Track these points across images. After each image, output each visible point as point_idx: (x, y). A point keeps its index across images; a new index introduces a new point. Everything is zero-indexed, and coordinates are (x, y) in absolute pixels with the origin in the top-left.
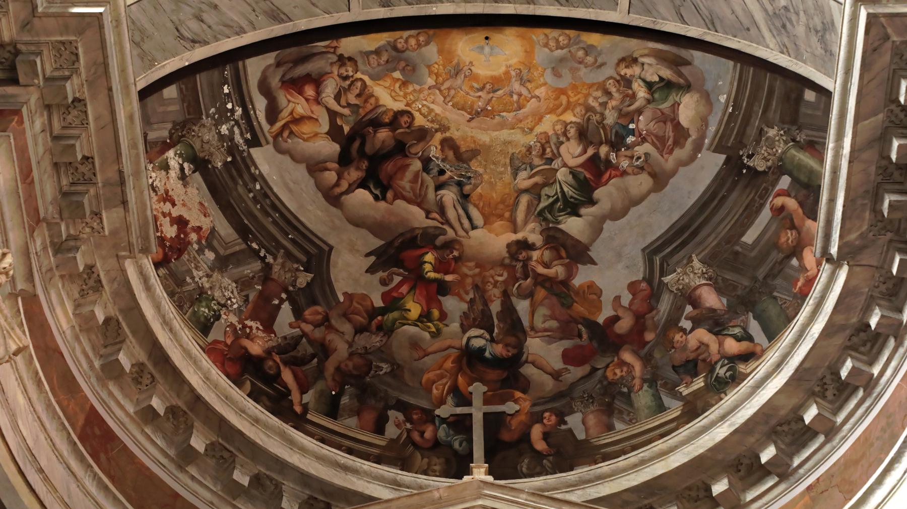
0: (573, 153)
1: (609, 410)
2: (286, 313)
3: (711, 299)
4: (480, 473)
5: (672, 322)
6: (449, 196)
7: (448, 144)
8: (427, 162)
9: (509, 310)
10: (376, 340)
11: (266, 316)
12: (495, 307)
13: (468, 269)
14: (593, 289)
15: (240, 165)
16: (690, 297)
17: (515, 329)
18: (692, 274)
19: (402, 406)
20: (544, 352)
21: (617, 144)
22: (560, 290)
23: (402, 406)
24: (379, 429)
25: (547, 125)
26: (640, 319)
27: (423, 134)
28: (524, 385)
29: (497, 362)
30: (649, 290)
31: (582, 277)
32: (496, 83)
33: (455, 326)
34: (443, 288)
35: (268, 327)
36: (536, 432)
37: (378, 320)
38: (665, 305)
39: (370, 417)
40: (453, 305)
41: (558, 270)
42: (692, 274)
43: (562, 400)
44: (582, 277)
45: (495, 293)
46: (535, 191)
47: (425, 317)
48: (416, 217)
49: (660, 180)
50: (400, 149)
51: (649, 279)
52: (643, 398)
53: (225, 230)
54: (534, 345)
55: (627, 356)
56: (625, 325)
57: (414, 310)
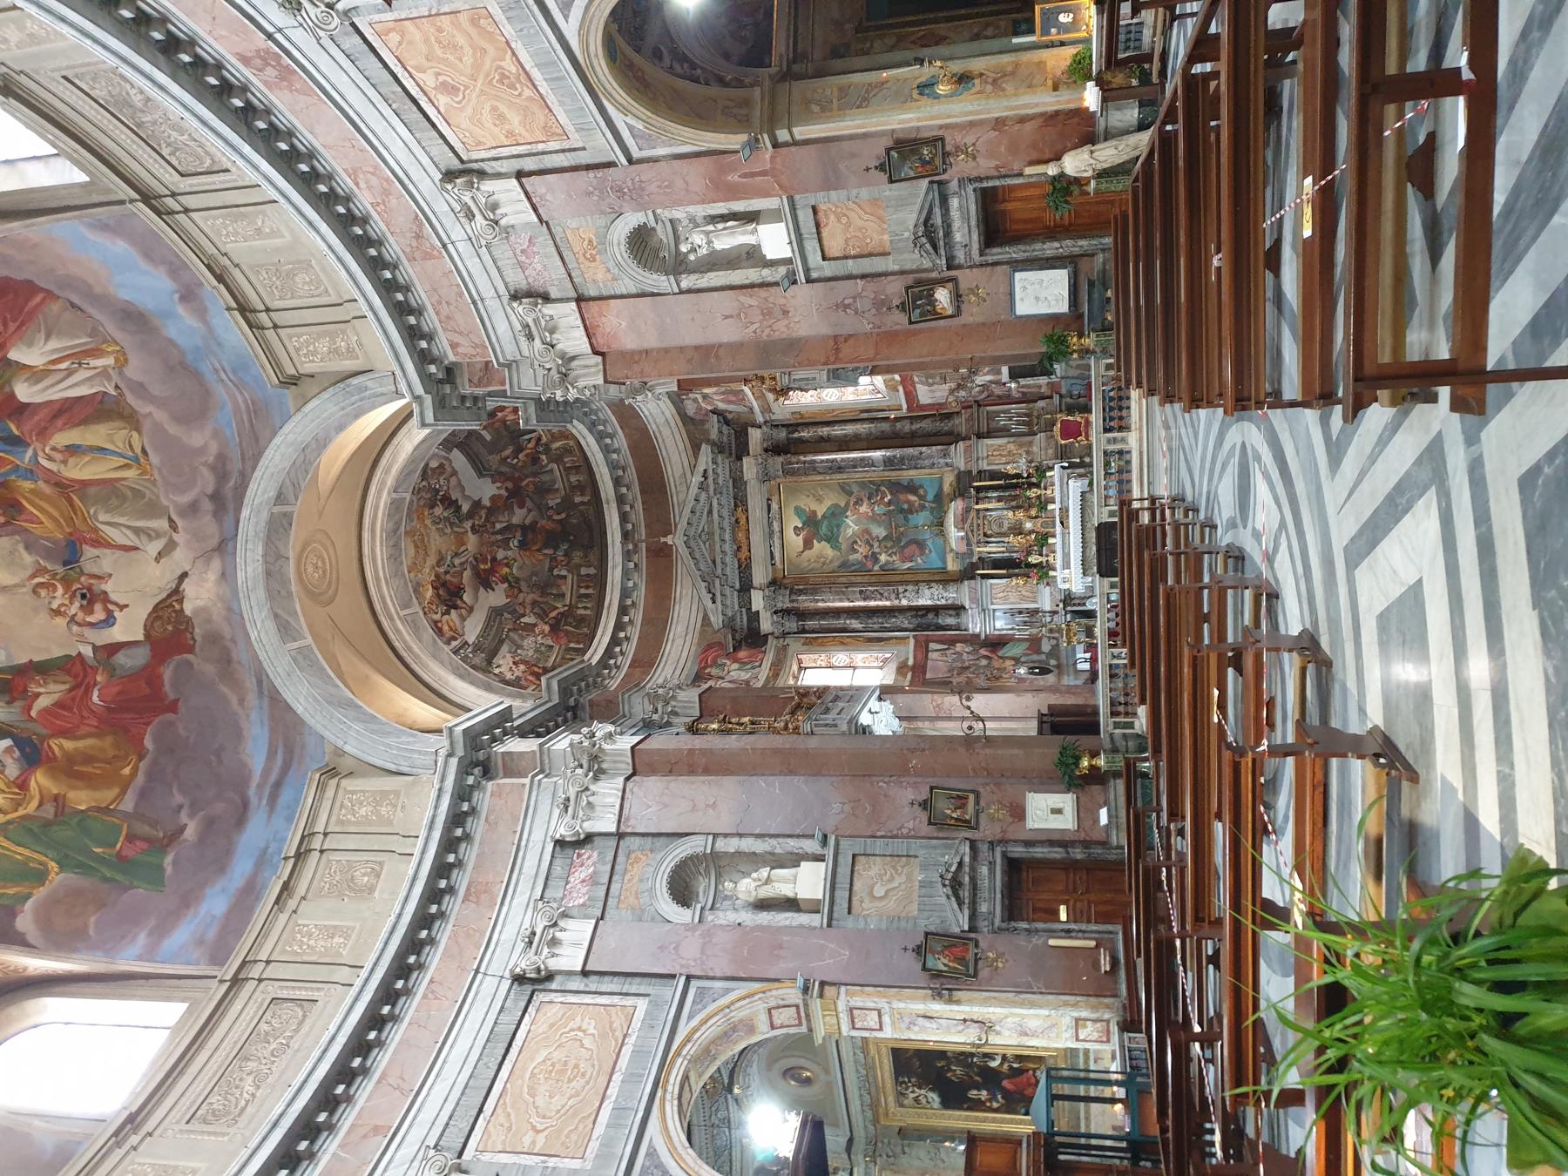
0: (438, 511)
3: (508, 452)
4: (669, 540)
5: (513, 466)
6: (457, 561)
7: (438, 564)
8: (446, 572)
9: (500, 532)
10: (523, 585)
11: (530, 628)
12: (499, 537)
13: (484, 550)
14: (493, 498)
15: (477, 648)
17: (509, 528)
18: (493, 460)
19: (551, 569)
20: (519, 516)
21: (437, 491)
22: (491, 511)
23: (551, 569)
24: (565, 577)
25: (428, 522)
26: (507, 479)
27: (437, 576)
28: (535, 523)
29: (524, 535)
30: (496, 476)
31: (487, 503)
32: (416, 546)
34: (494, 559)
35: (535, 625)
36: (556, 517)
37: (514, 585)
38: (504, 469)
39: (560, 582)
40: (500, 555)
41: (483, 513)
42: (493, 460)
43: (542, 508)
44: (487, 503)
45: (493, 538)
46: (452, 524)
47: (507, 565)
48: (467, 574)
49: (454, 473)
50: (444, 584)
51: (492, 476)
52: (545, 478)
53: (505, 648)
54: (515, 520)
56: (510, 485)
57: (506, 570)
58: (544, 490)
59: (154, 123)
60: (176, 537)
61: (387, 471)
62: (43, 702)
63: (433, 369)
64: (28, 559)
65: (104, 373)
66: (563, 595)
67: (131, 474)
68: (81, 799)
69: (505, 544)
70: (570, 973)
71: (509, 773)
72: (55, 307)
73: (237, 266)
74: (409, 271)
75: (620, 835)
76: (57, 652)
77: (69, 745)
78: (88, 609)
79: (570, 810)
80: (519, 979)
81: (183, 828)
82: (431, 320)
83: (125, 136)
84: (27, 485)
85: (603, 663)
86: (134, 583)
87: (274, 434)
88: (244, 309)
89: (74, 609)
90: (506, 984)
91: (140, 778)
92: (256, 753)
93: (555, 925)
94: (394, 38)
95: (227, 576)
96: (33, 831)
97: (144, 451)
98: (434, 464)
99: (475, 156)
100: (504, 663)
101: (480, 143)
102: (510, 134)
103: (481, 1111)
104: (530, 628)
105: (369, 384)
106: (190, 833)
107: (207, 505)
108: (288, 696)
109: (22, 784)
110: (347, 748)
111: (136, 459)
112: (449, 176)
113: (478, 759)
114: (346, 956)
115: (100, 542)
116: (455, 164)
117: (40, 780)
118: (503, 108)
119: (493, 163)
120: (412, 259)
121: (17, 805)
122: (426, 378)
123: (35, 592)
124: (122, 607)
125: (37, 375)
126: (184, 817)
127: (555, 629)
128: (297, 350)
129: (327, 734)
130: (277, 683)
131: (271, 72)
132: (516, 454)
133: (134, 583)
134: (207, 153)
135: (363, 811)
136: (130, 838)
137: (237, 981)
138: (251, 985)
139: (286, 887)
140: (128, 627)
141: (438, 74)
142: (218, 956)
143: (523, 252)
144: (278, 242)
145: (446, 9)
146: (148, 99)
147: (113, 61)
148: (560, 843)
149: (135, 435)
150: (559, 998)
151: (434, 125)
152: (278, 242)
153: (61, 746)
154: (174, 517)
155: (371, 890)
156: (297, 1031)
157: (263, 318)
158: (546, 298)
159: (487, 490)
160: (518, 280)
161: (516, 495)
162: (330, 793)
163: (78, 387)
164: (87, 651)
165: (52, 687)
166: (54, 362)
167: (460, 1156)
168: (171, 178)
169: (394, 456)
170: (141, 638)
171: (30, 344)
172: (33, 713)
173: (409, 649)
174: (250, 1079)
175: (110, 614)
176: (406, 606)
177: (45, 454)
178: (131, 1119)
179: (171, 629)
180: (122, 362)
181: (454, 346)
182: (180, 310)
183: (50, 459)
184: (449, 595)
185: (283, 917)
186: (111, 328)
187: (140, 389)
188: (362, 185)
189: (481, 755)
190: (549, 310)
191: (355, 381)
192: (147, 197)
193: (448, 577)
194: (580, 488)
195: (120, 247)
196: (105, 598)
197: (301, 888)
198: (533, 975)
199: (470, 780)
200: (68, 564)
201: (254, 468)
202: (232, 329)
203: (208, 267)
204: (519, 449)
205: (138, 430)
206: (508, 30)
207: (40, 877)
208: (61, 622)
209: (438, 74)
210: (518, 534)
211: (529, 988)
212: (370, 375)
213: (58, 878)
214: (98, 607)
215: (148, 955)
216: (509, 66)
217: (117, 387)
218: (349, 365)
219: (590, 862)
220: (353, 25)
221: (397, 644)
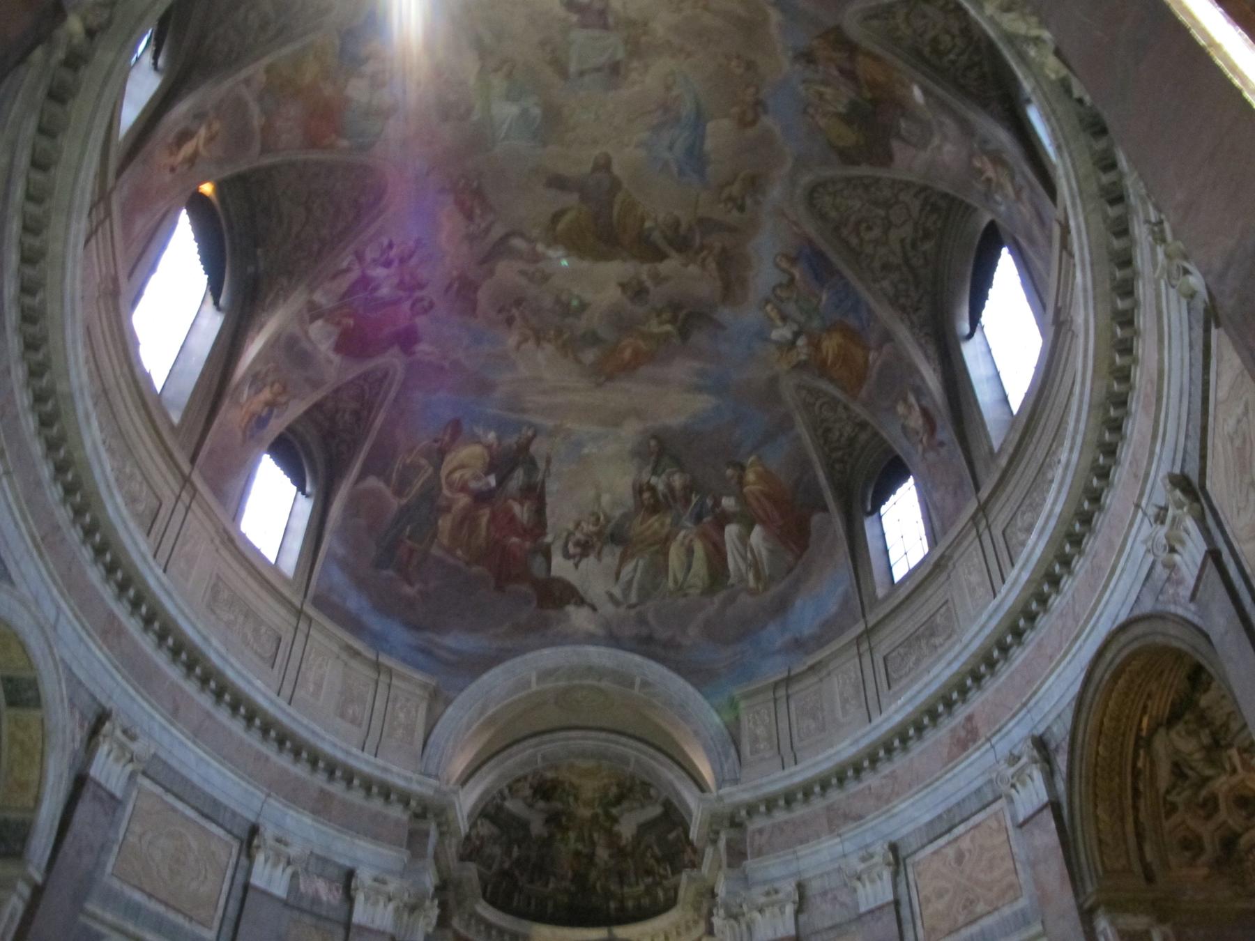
0: (614, 790)
1: (622, 883)
2: (516, 849)
3: (656, 850)
6: (571, 799)
8: (564, 790)
9: (591, 836)
12: (586, 835)
14: (619, 836)
15: (500, 808)
16: (649, 847)
17: (593, 844)
20: (602, 854)
25: (606, 781)
31: (616, 828)
33: (572, 841)
34: (568, 829)
36: (598, 885)
37: (547, 842)
38: (642, 846)
40: (572, 835)
41: (607, 824)
49: (643, 806)
53: (495, 830)
55: (630, 860)
56: (629, 849)
58: (622, 877)
59: (920, 647)
60: (622, 610)
61: (652, 757)
62: (517, 508)
63: (743, 813)
64: (617, 513)
65: (743, 579)
66: (531, 881)
67: (671, 584)
68: (445, 523)
69: (580, 839)
70: (249, 872)
71: (412, 834)
72: (790, 558)
73: (821, 680)
74: (818, 804)
75: (348, 925)
76: (550, 522)
77: (484, 521)
78: (577, 544)
79: (376, 884)
80: (254, 830)
81: (411, 584)
82: (780, 816)
83: (910, 627)
84: (668, 521)
85: (474, 915)
86: (593, 576)
87: (695, 685)
88: (789, 681)
89: (579, 536)
90: (251, 817)
91: (451, 560)
92: (456, 641)
93: (289, 863)
94: (994, 825)
95: (591, 639)
96: (430, 494)
97: (685, 595)
98: (653, 792)
99: (910, 869)
100: (485, 829)
101: (919, 875)
102: (928, 900)
103: (167, 790)
104: (508, 852)
105: (730, 761)
106: (408, 590)
107: (644, 631)
108: (497, 670)
109: (464, 488)
110: (450, 710)
111: (681, 588)
112: (894, 848)
113: (427, 811)
114: (300, 693)
115: (623, 559)
116: (902, 853)
117: (463, 500)
118: (947, 898)
119: (904, 882)
120: (829, 808)
121: (451, 485)
122: (737, 807)
123: (593, 514)
124: (576, 566)
125: (744, 539)
126: (418, 586)
127: (504, 874)
128: (758, 713)
129: (464, 694)
130: (508, 664)
131: (963, 734)
132: (654, 856)
133: (593, 576)
134: (901, 677)
135: (402, 715)
136: (411, 551)
137: (299, 613)
138: (293, 621)
139: (356, 654)
140: (561, 567)
141: (970, 851)
142: (322, 603)
143: (835, 898)
144: (839, 714)
145: (1018, 866)
146: (936, 647)
147: (965, 639)
148: (350, 874)
149: (698, 591)
150: (233, 860)
151: (931, 842)
152: (839, 714)
153: (485, 515)
154: (638, 608)
155: (342, 716)
156: (256, 653)
157: (781, 692)
158: (798, 912)
159: (627, 828)
160: (814, 887)
161: (619, 852)
162: (419, 691)
163: (733, 561)
164: (549, 539)
165: (526, 516)
166: (752, 551)
167: (144, 773)
168: (883, 649)
169: (662, 764)
170: (553, 573)
171: (765, 539)
172: (510, 502)
173: (511, 756)
174: (232, 617)
175: (573, 557)
176: (544, 757)
177: (687, 532)
178: (231, 540)
179: (558, 595)
180: (753, 593)
181: (761, 831)
182: (788, 636)
183: (685, 537)
184: (545, 790)
185: (335, 649)
186: (775, 590)
187: (731, 600)
188: (884, 781)
189: (430, 815)
190: (790, 909)
191: (733, 751)
192: (869, 632)
193: (559, 790)
194: (622, 908)
195: (833, 607)
196: (584, 555)
197: (354, 663)
198: (256, 842)
199: (413, 803)
200: (611, 536)
201: (670, 667)
202: (774, 670)
203: (820, 662)
204: (658, 861)
205: (703, 593)
206: (1007, 911)
207: (399, 493)
208: (571, 526)
209: (970, 851)
210: (585, 851)
211: (245, 836)
212: (737, 762)
213: (395, 503)
214: (578, 550)
215: (331, 555)
216: (980, 908)
217: (733, 585)
218: (746, 749)
219: (331, 897)
220: (1000, 797)
221: (515, 748)
